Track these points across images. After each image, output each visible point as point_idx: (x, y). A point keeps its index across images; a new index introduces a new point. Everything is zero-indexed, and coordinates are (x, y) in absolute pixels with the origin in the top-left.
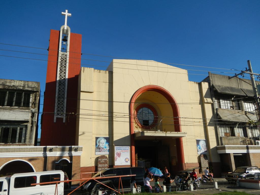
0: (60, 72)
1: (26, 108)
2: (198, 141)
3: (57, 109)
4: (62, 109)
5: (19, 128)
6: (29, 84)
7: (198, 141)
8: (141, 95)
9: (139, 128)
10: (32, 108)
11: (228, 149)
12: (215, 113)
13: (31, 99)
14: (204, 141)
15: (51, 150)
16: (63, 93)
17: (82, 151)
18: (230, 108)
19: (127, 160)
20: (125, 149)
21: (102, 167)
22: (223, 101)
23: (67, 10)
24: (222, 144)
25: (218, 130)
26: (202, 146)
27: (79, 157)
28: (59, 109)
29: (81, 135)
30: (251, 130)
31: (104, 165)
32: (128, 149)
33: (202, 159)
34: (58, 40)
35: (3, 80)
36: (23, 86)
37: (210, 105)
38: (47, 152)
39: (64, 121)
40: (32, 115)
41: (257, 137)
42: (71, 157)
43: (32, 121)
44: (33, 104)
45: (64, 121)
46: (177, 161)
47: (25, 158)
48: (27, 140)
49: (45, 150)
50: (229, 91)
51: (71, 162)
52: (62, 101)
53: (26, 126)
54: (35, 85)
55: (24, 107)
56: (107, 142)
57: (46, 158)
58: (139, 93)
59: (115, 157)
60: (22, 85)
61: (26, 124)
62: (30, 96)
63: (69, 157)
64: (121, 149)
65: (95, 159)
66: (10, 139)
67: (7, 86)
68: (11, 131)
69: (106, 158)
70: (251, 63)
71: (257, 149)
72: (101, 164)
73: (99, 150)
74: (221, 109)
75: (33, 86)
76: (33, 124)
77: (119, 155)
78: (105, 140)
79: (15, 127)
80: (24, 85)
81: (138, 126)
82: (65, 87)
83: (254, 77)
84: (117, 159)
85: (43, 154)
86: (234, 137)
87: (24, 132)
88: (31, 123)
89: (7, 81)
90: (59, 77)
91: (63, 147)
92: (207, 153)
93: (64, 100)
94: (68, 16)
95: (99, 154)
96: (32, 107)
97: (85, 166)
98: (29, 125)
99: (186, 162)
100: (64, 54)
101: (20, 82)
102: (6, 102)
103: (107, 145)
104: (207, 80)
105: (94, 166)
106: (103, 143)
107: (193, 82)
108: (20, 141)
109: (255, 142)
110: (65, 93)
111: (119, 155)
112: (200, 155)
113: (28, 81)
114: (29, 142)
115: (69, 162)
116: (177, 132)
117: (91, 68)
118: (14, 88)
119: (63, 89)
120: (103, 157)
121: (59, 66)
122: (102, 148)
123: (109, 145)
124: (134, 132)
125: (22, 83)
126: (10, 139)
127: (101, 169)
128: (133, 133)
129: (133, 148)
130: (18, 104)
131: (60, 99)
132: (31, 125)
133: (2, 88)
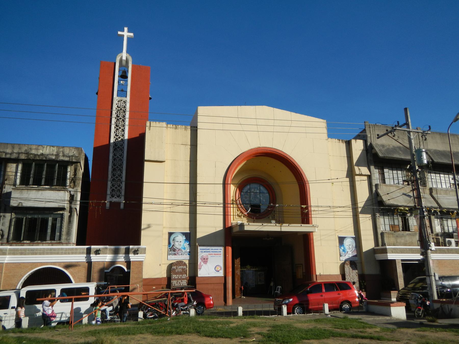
0: (116, 129)
1: (61, 187)
2: (341, 240)
3: (111, 188)
4: (119, 188)
5: (50, 219)
6: (65, 151)
7: (341, 240)
8: (245, 164)
9: (243, 217)
10: (71, 187)
11: (392, 252)
12: (374, 192)
13: (69, 174)
14: (352, 239)
15: (97, 252)
16: (120, 162)
17: (145, 253)
18: (402, 183)
20: (215, 252)
21: (178, 279)
22: (391, 172)
23: (126, 27)
24: (383, 244)
25: (377, 220)
26: (349, 247)
27: (141, 263)
28: (114, 188)
29: (144, 229)
30: (440, 221)
31: (181, 275)
32: (220, 250)
33: (348, 268)
34: (112, 77)
35: (27, 146)
36: (56, 155)
37: (366, 178)
38: (91, 255)
39: (122, 206)
40: (70, 198)
41: (451, 233)
42: (128, 263)
43: (71, 208)
44: (72, 182)
45: (122, 206)
46: (304, 271)
47: (59, 263)
48: (64, 237)
49: (89, 252)
50: (399, 154)
51: (129, 270)
52: (119, 176)
53: (62, 216)
54: (73, 152)
55: (59, 186)
56: (186, 240)
57: (90, 263)
58: (240, 161)
59: (199, 263)
60: (55, 153)
61: (61, 212)
62: (67, 169)
63: (126, 263)
64: (208, 251)
65: (168, 267)
66: (37, 234)
67: (31, 155)
68: (39, 223)
69: (185, 264)
70: (410, 112)
71: (446, 253)
72: (176, 274)
73: (173, 252)
74: (384, 184)
75: (71, 154)
76: (72, 213)
77: (205, 260)
78: (183, 237)
79: (45, 216)
80: (58, 153)
81: (242, 213)
82: (123, 153)
83: (414, 135)
84: (202, 267)
85: (86, 257)
86: (407, 232)
87: (58, 225)
88: (69, 210)
89: (32, 148)
90: (114, 137)
91: (115, 248)
92: (356, 258)
93: (121, 174)
94: (129, 37)
95: (174, 258)
96: (71, 186)
97: (150, 277)
98: (66, 214)
99: (318, 273)
100: (121, 100)
101: (52, 148)
102: (31, 180)
103: (186, 245)
104: (362, 136)
105: (166, 276)
106: (180, 242)
107: (336, 140)
108: (52, 238)
109: (444, 240)
110: (123, 162)
111: (206, 260)
112: (344, 262)
113: (63, 147)
114: (67, 239)
115: (126, 270)
117: (162, 123)
118: (43, 158)
119: (120, 155)
120: (180, 263)
121: (114, 120)
122: (179, 250)
123: (190, 245)
124: (232, 224)
125: (54, 150)
126: (37, 234)
127: (176, 281)
128: (230, 225)
129: (230, 249)
130: (50, 183)
131: (115, 172)
132: (69, 214)
133: (26, 158)
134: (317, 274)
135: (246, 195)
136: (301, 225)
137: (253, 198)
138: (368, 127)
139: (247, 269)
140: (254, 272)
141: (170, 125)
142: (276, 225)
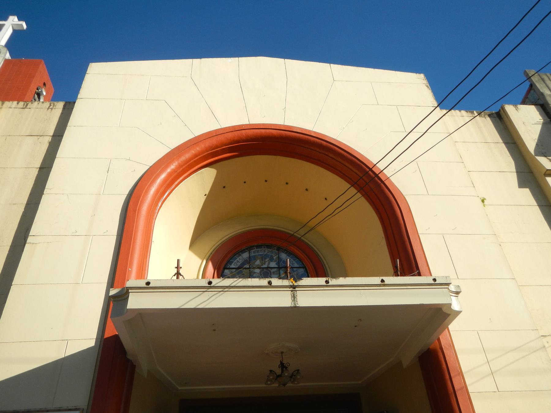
94: (16, 28)
136: (383, 281)
138: (537, 79)
141: (11, 102)
142: (270, 283)
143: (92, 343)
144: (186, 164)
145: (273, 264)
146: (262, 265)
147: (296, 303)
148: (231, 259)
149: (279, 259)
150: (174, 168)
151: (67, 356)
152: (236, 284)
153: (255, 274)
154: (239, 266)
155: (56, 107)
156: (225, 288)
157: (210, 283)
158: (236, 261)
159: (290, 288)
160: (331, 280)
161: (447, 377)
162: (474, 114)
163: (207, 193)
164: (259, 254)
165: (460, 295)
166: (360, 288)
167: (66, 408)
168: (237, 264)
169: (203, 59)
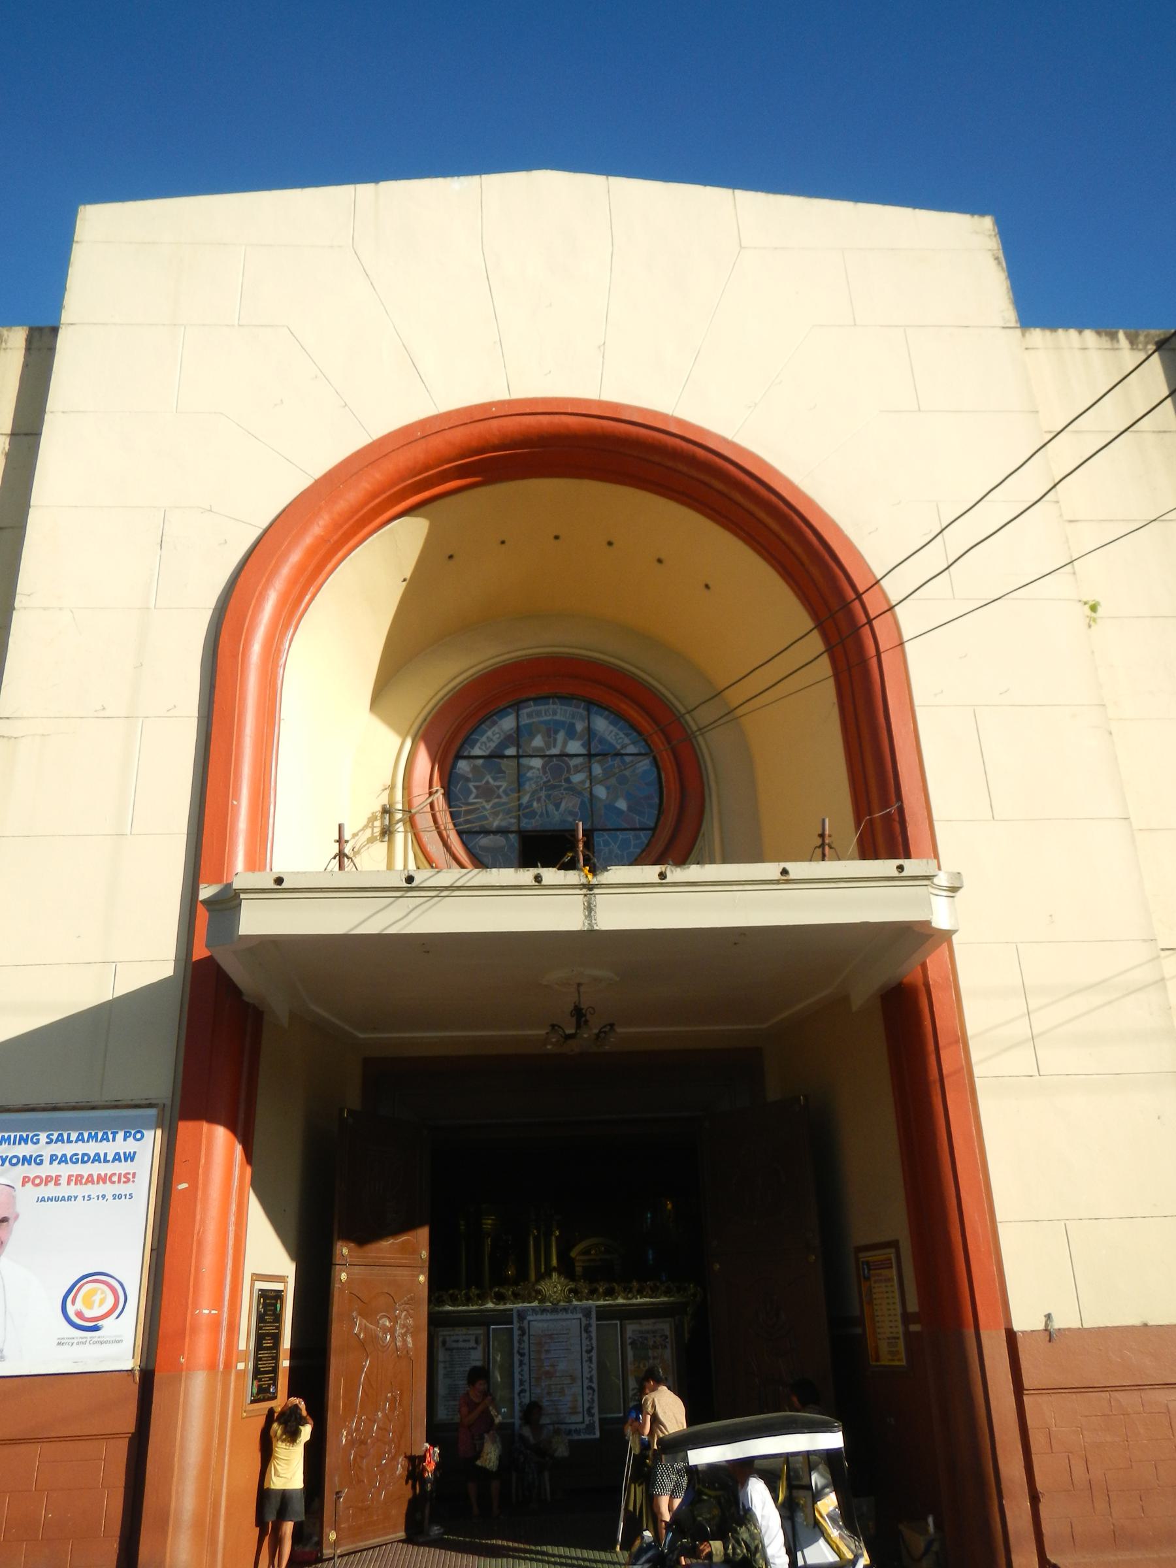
19: (96, 1301)
20: (85, 1159)
46: (913, 1306)
99: (1025, 1319)
116: (770, 870)
134: (1017, 1326)
135: (489, 778)
136: (785, 872)
137: (543, 794)
139: (541, 1301)
140: (594, 1322)
142: (538, 878)
143: (167, 970)
144: (349, 518)
145: (575, 747)
146: (549, 749)
147: (593, 921)
148: (472, 734)
149: (590, 732)
150: (322, 533)
151: (120, 997)
152: (466, 883)
153: (531, 771)
154: (492, 751)
155: (9, 345)
156: (442, 891)
157: (410, 879)
158: (484, 739)
159: (581, 889)
160: (672, 871)
161: (931, 1047)
162: (1118, 341)
163: (408, 576)
164: (542, 719)
165: (959, 894)
166: (735, 888)
167: (129, 1103)
168: (488, 745)
169: (384, 185)
